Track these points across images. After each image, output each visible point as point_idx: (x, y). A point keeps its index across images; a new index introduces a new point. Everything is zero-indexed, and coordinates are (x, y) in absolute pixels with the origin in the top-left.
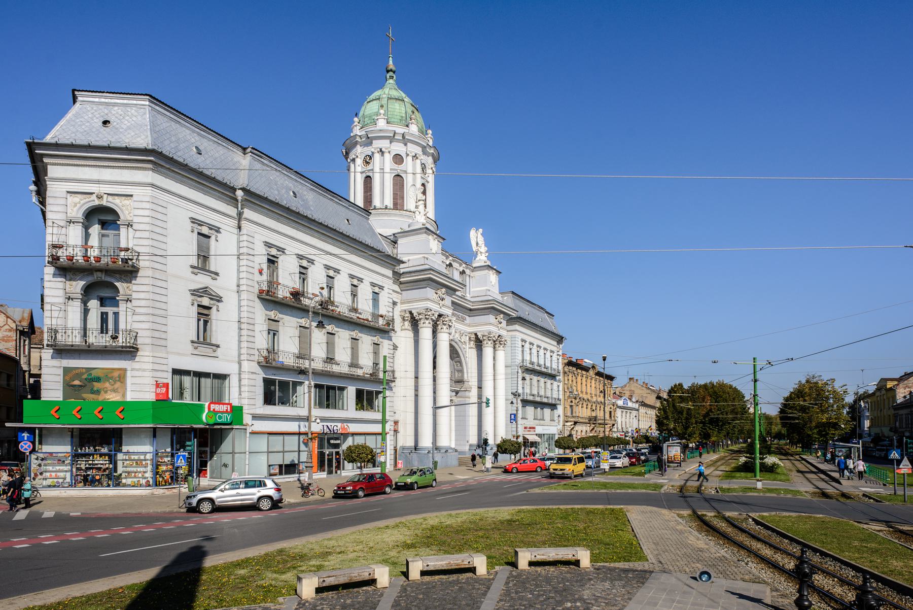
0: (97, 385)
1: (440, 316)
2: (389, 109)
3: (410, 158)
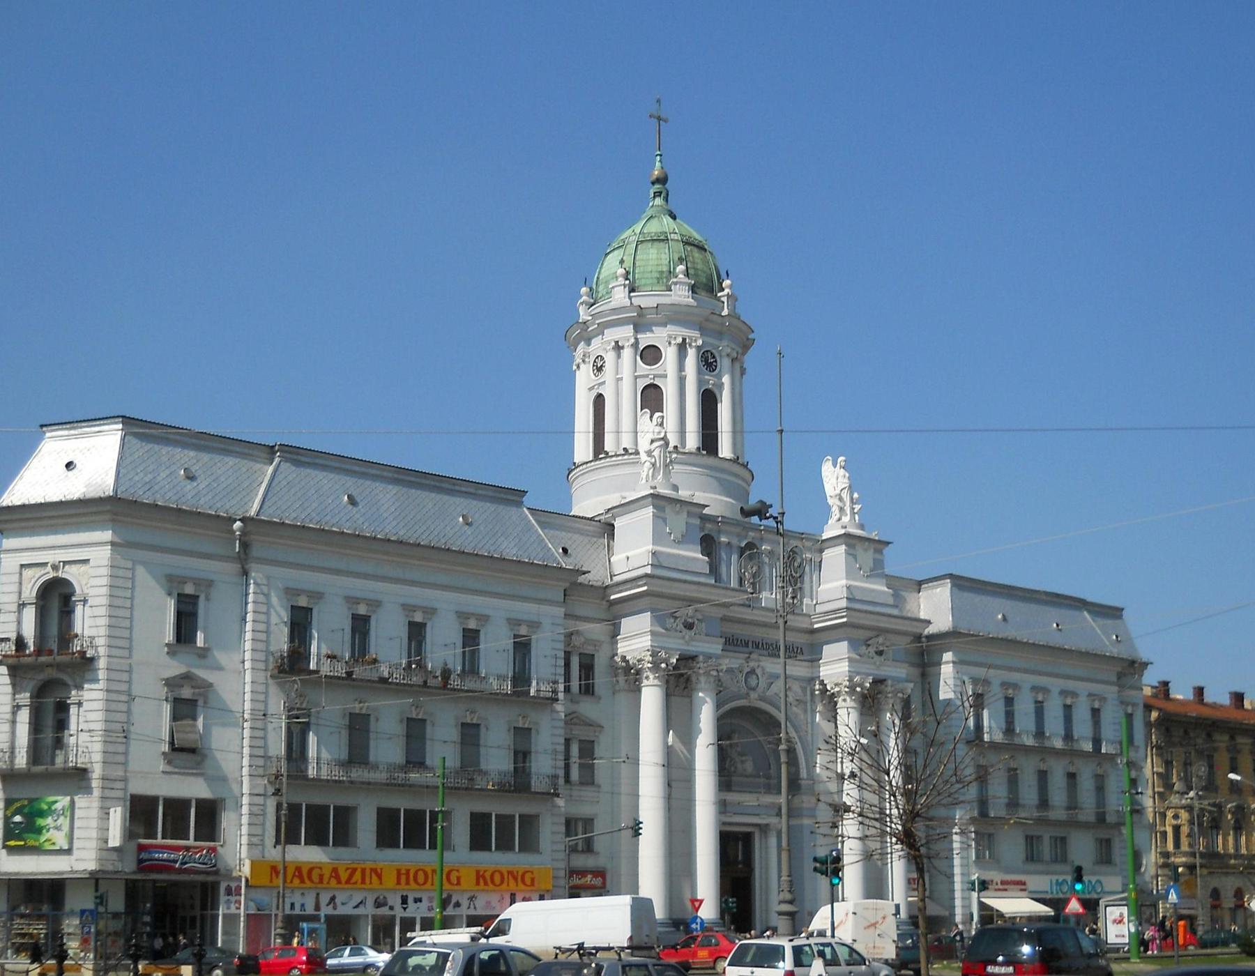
2: (637, 263)
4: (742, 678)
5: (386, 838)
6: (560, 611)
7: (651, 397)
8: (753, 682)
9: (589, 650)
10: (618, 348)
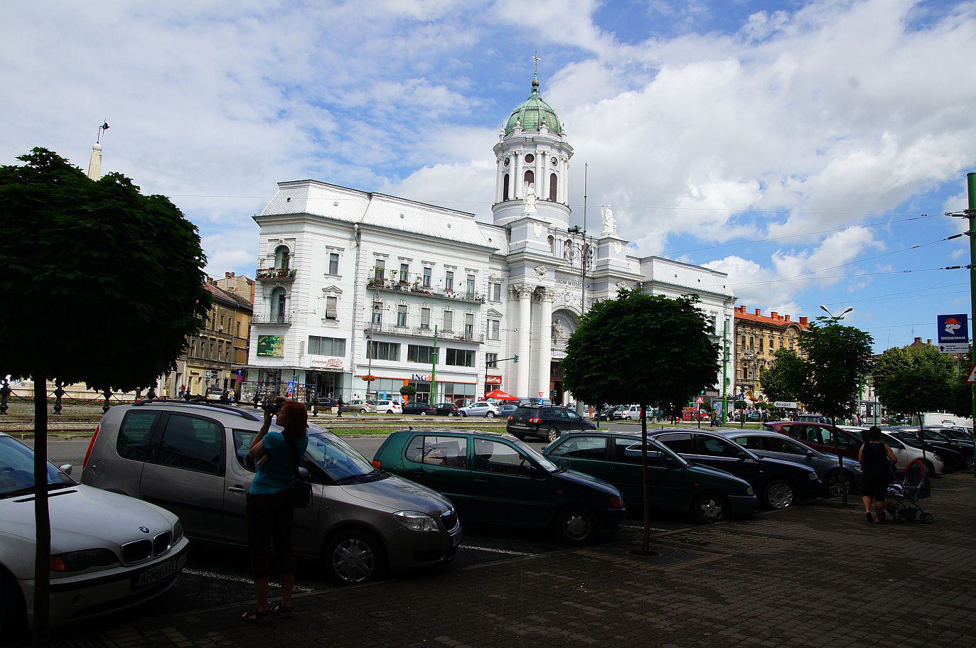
0: (272, 345)
1: (539, 287)
3: (540, 157)
4: (563, 297)
5: (412, 357)
6: (487, 266)
7: (529, 177)
8: (567, 298)
9: (499, 282)
10: (516, 155)
